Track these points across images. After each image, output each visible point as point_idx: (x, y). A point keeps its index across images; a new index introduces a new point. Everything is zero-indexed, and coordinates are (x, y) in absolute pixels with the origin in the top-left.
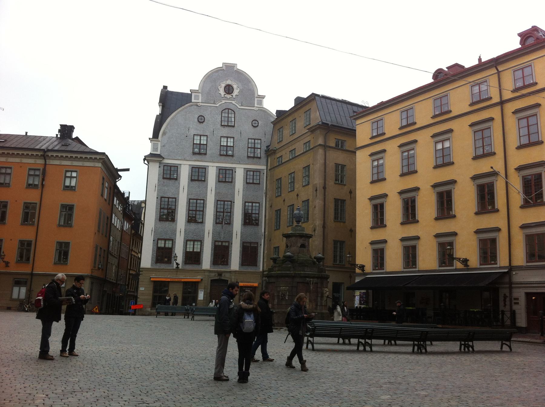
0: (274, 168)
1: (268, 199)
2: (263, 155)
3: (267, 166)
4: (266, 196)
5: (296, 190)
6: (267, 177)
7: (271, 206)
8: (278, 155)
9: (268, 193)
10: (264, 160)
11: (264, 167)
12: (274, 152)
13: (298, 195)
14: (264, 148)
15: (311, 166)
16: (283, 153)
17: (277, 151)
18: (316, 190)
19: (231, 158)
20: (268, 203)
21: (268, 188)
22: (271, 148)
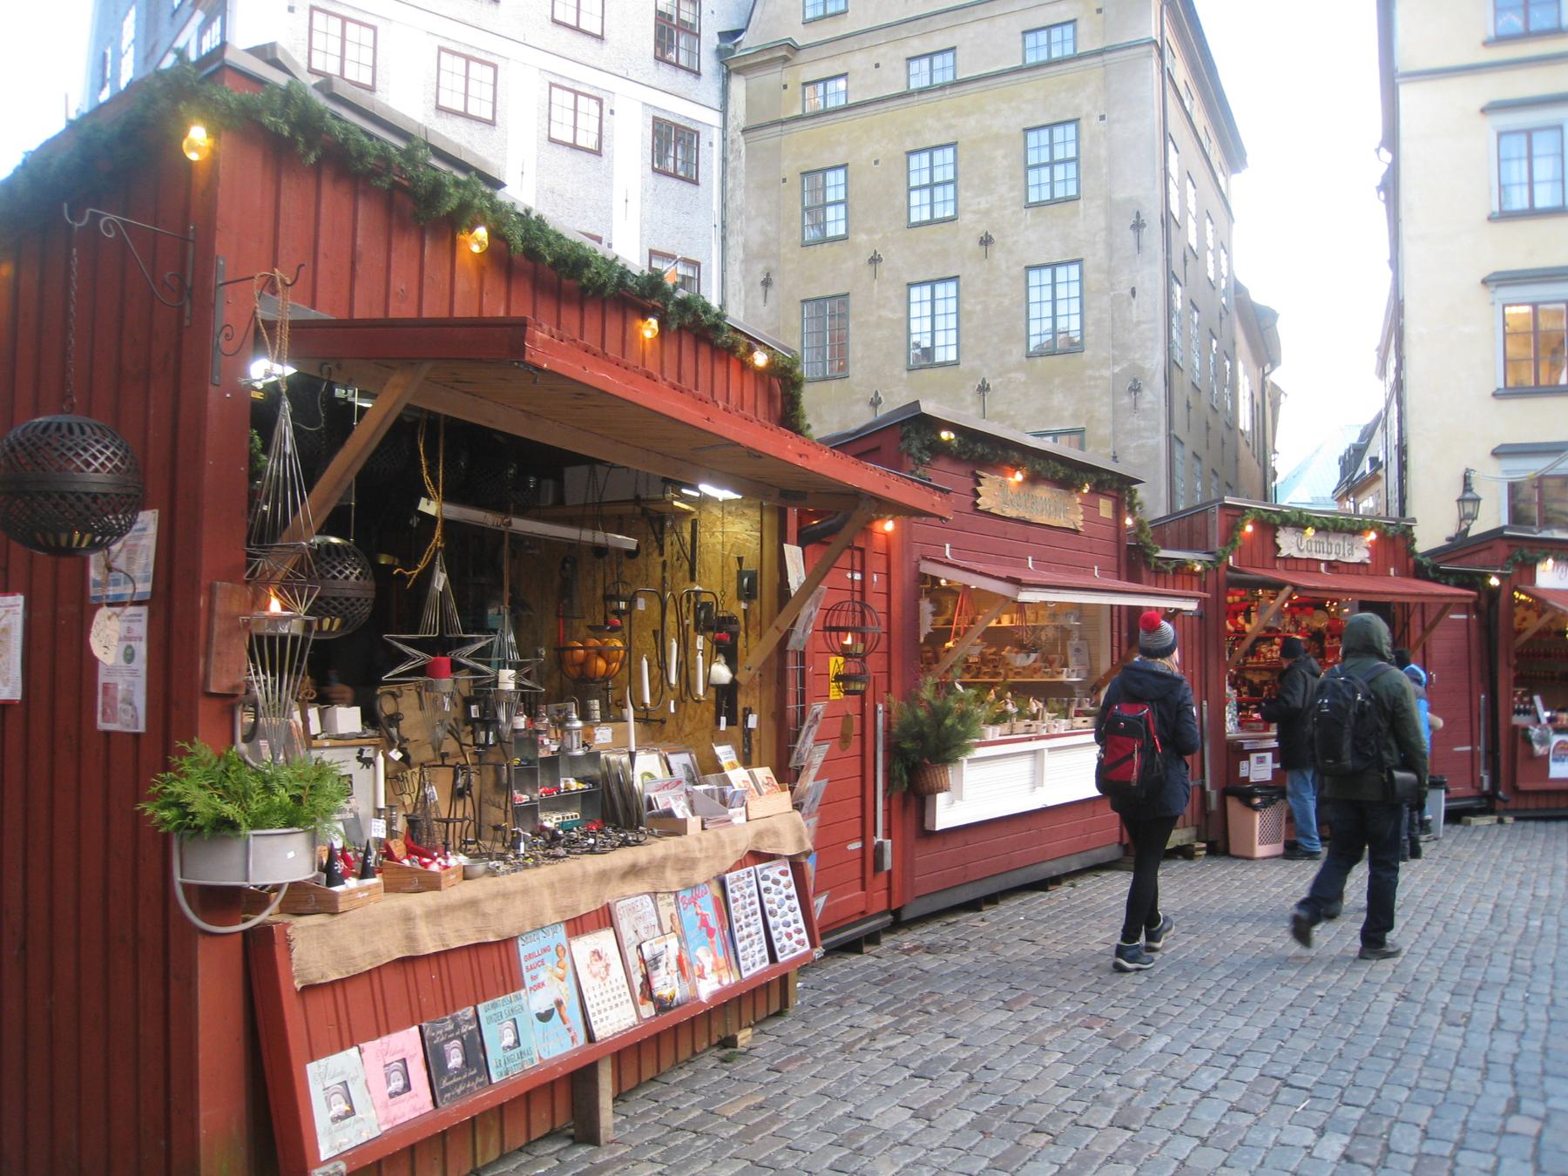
0: (782, 122)
1: (736, 252)
2: (708, 63)
3: (724, 110)
4: (724, 238)
5: (966, 219)
6: (724, 160)
7: (767, 283)
8: (809, 73)
9: (735, 225)
10: (709, 87)
11: (715, 118)
12: (787, 53)
13: (986, 241)
14: (710, 40)
15: (1090, 125)
16: (857, 62)
17: (803, 56)
18: (1138, 226)
19: (593, 42)
20: (735, 269)
21: (738, 199)
22: (748, 41)
